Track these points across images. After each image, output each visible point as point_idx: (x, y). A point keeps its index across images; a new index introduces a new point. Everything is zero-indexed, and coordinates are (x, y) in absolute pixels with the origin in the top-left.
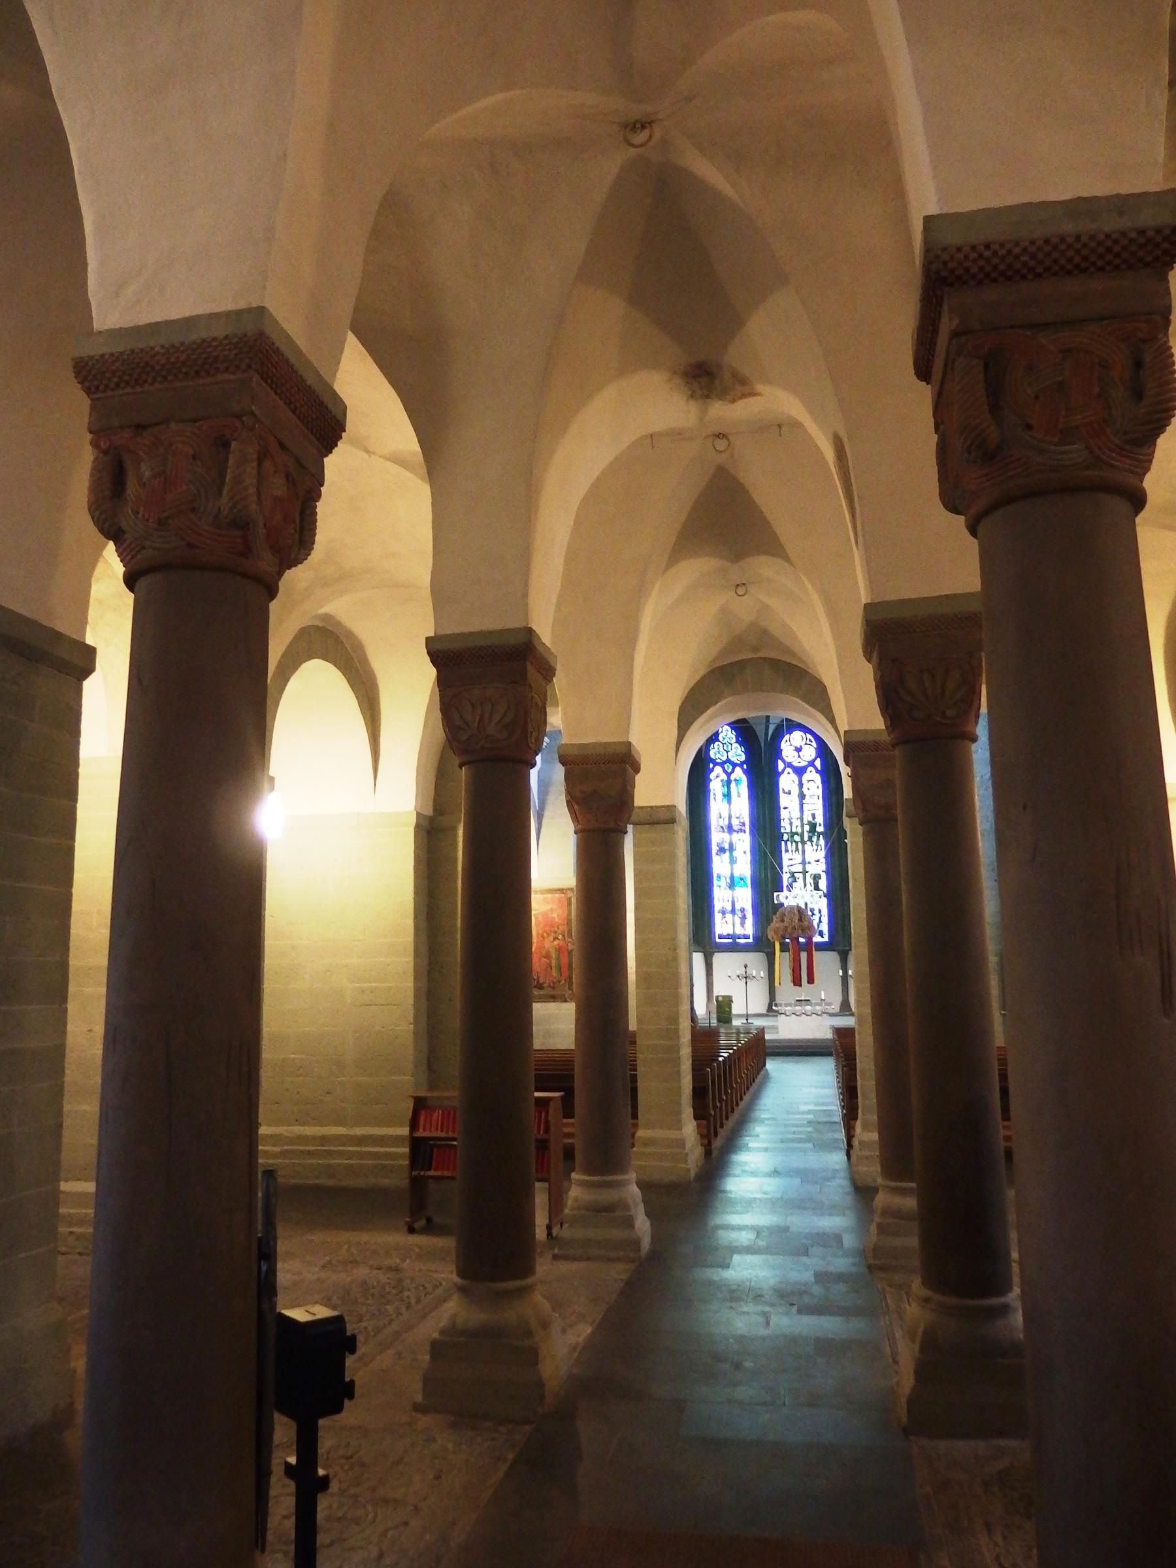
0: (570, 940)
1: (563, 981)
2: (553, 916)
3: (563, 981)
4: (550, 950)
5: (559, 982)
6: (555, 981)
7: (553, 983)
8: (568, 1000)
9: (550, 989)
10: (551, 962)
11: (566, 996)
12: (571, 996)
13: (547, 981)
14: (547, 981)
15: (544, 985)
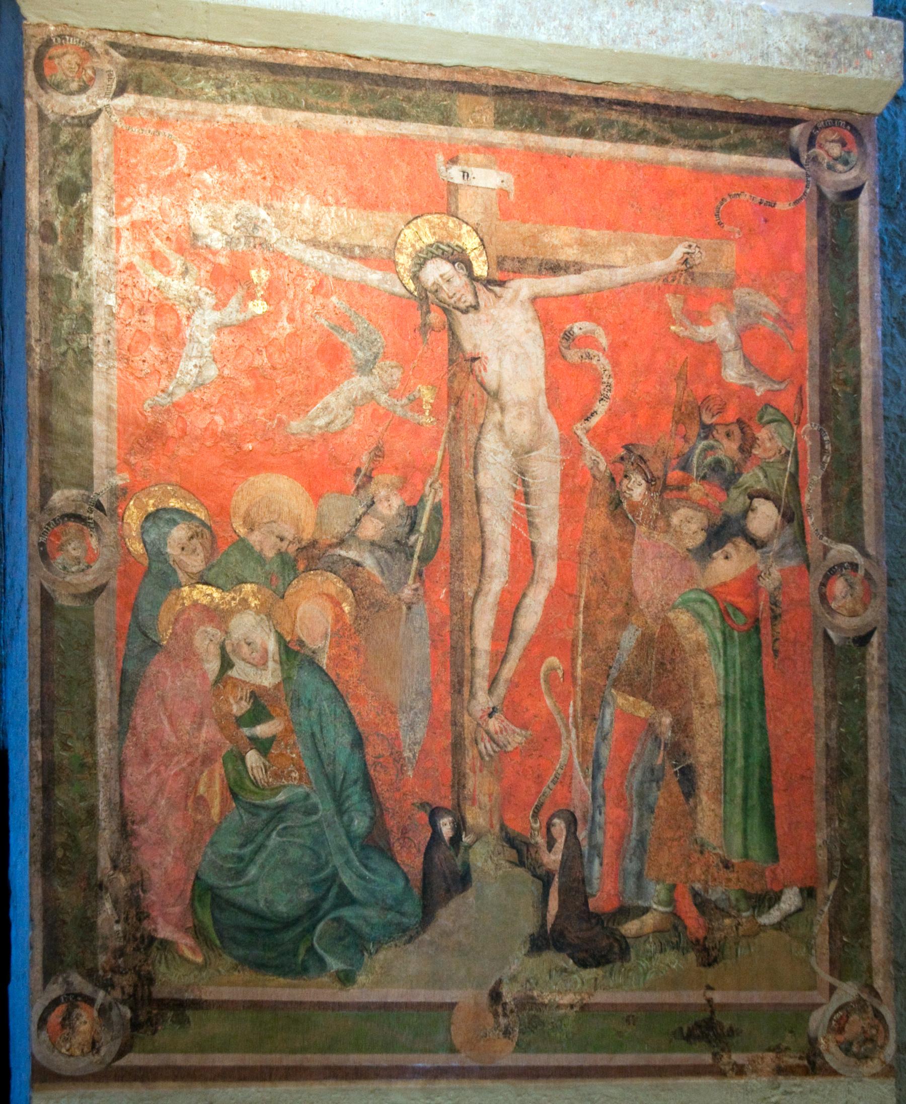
0: (843, 551)
1: (790, 900)
2: (704, 332)
3: (790, 900)
4: (682, 620)
5: (770, 899)
6: (715, 894)
7: (702, 904)
8: (833, 1056)
9: (672, 960)
10: (682, 726)
11: (817, 1021)
12: (856, 1024)
13: (656, 892)
14: (656, 892)
15: (631, 928)
